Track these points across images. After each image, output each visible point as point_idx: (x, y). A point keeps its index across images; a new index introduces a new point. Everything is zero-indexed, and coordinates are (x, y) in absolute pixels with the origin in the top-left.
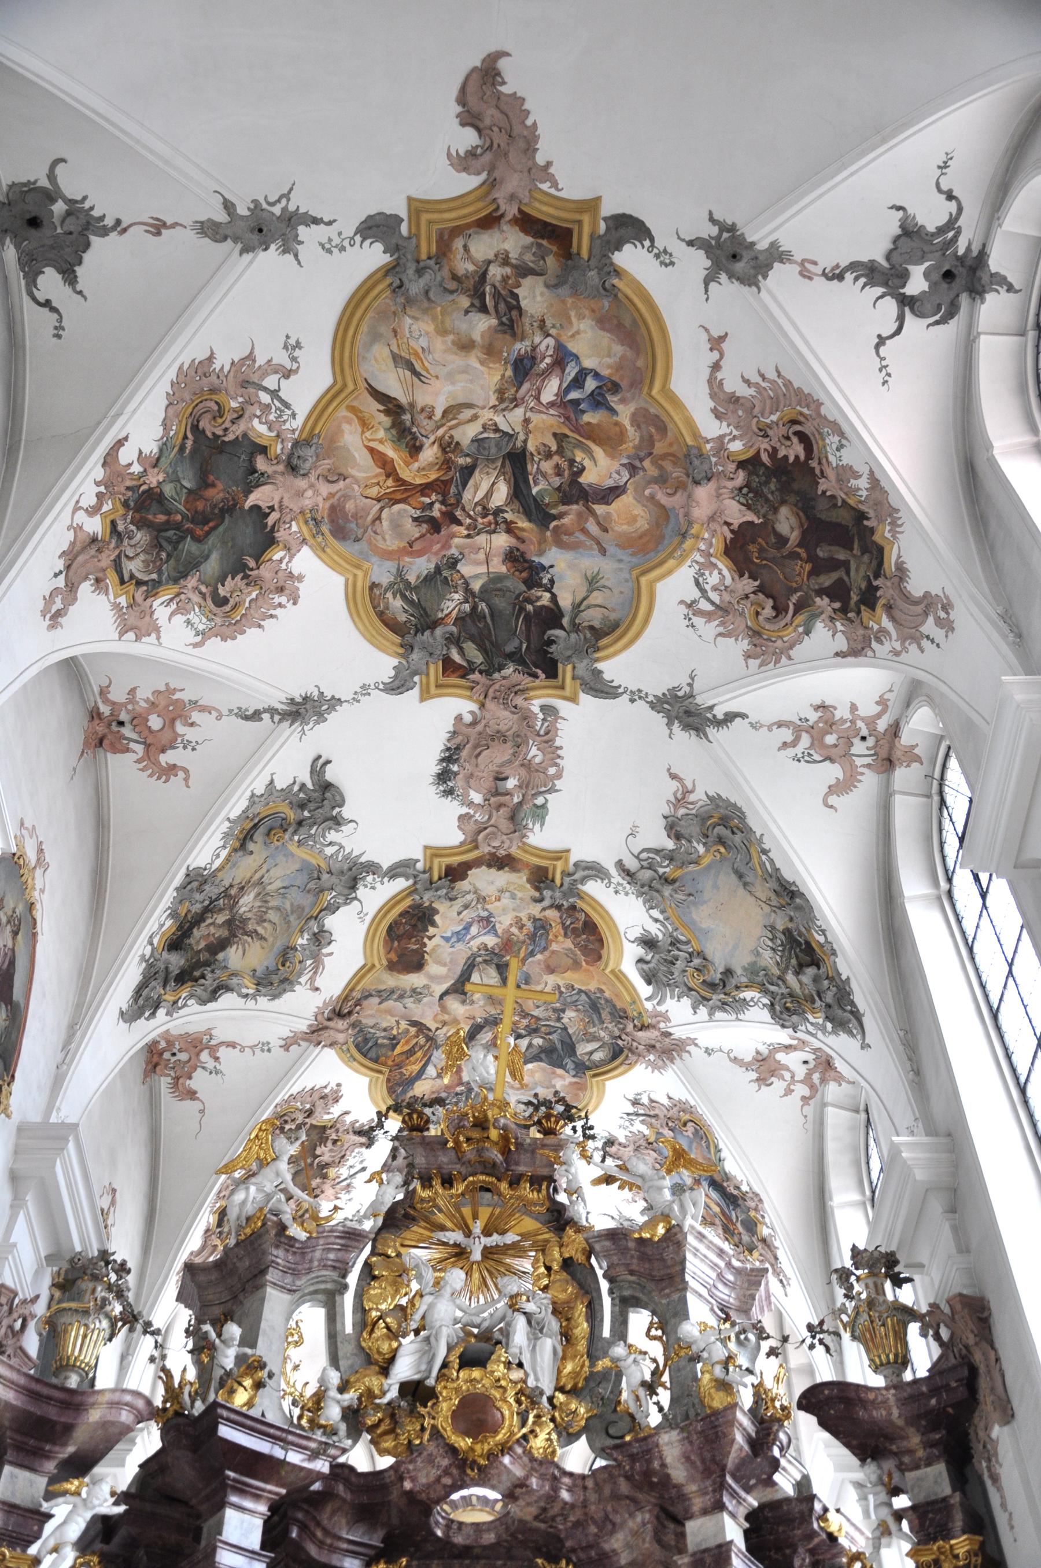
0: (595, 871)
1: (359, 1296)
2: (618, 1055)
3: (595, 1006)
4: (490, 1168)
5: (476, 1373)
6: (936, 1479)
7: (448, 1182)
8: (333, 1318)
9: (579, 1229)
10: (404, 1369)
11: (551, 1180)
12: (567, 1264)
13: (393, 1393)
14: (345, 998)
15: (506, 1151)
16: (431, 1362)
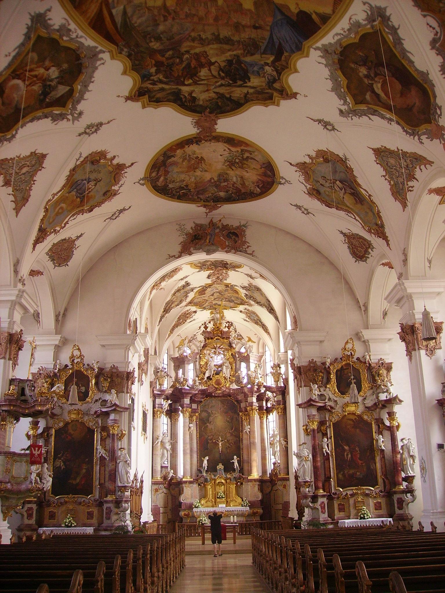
0: (236, 286)
1: (199, 362)
2: (242, 304)
3: (237, 298)
4: (219, 336)
5: (218, 376)
6: (280, 397)
7: (212, 338)
8: (195, 365)
9: (234, 349)
10: (207, 375)
11: (229, 338)
12: (232, 354)
13: (206, 379)
14: (191, 301)
15: (221, 333)
16: (211, 372)
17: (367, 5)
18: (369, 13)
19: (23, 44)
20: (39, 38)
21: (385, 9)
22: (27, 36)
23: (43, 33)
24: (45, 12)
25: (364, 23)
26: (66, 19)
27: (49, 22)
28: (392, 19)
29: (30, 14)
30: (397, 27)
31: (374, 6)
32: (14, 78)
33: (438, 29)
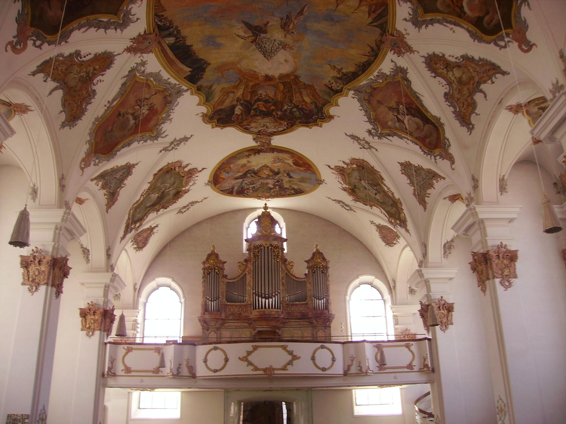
17: (136, 20)
18: (130, 17)
19: (439, 22)
20: (426, 11)
21: (122, 31)
22: (432, 22)
23: (420, 11)
24: (409, 21)
25: (130, 7)
26: (399, 3)
27: (412, 13)
28: (114, 31)
29: (419, 31)
30: (107, 31)
31: (131, 24)
32: (465, 13)
33: (84, 59)
